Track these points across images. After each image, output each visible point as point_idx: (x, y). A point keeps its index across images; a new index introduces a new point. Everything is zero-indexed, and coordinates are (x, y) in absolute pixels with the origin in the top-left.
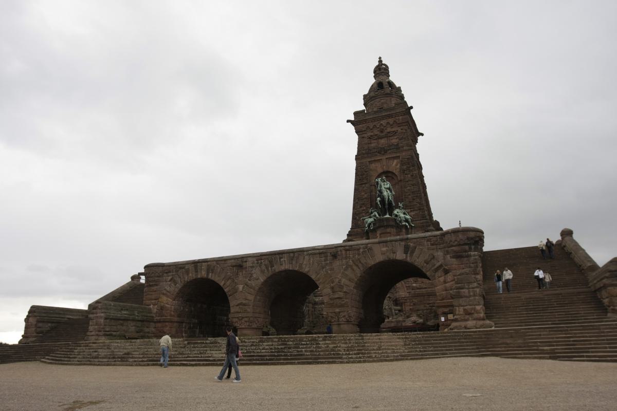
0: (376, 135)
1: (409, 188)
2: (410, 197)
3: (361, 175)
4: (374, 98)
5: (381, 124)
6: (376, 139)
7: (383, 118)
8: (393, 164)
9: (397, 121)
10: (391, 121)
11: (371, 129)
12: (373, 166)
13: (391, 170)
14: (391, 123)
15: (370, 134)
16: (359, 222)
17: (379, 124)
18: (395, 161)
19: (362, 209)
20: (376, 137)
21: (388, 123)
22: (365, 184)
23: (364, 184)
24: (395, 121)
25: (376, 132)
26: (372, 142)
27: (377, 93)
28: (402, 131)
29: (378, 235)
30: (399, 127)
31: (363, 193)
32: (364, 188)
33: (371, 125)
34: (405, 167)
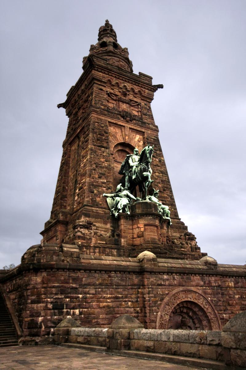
0: (116, 95)
1: (157, 174)
2: (160, 185)
3: (99, 134)
4: (111, 54)
5: (125, 86)
6: (115, 100)
8: (135, 138)
11: (113, 86)
13: (132, 145)
14: (136, 91)
15: (109, 90)
16: (98, 199)
17: (123, 85)
18: (138, 137)
20: (115, 98)
21: (132, 89)
22: (107, 148)
23: (104, 147)
25: (116, 91)
26: (110, 101)
28: (145, 106)
30: (142, 99)
31: (102, 160)
32: (104, 153)
33: (114, 81)
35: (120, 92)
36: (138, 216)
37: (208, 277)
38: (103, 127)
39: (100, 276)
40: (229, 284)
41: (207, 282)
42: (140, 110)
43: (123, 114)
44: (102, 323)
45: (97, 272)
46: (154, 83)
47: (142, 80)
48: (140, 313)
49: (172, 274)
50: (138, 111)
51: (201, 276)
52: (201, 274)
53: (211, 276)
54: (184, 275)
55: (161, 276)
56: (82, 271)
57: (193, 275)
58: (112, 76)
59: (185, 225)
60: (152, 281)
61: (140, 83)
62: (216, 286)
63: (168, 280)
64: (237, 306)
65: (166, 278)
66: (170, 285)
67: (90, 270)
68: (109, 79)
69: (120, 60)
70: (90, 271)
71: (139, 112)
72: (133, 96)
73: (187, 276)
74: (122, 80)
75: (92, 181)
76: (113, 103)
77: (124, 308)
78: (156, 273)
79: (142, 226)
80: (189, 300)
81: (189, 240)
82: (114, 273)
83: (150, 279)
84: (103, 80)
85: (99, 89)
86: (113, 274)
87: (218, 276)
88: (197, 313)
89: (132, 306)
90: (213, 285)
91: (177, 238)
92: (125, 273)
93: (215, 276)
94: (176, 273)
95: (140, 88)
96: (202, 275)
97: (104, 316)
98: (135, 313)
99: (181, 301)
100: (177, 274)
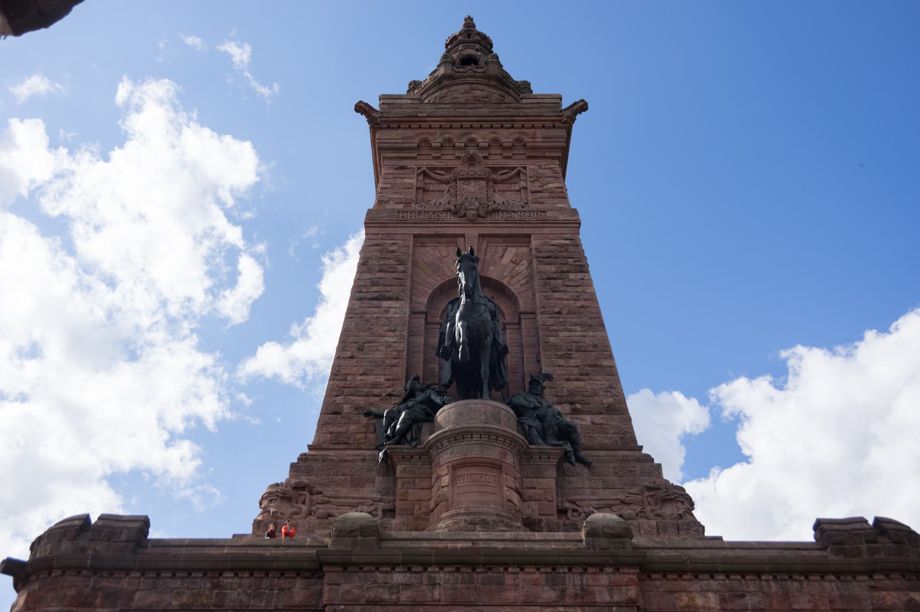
0: (448, 170)
5: (472, 140)
7: (481, 123)
8: (502, 257)
9: (527, 139)
10: (506, 136)
11: (436, 149)
12: (429, 253)
13: (493, 277)
15: (425, 163)
17: (464, 139)
18: (511, 252)
19: (370, 379)
20: (447, 177)
21: (496, 140)
23: (390, 299)
24: (519, 140)
25: (449, 160)
26: (431, 188)
27: (461, 70)
29: (443, 470)
32: (387, 311)
34: (552, 268)
35: (458, 158)
36: (437, 447)
37: (581, 573)
38: (392, 252)
39: (186, 585)
40: (693, 599)
41: (570, 591)
42: (523, 184)
43: (455, 206)
45: (178, 575)
46: (565, 104)
47: (529, 111)
49: (425, 570)
50: (519, 191)
51: (545, 573)
52: (546, 565)
53: (590, 570)
54: (474, 570)
55: (384, 575)
56: (133, 574)
57: (510, 570)
58: (430, 127)
59: (656, 462)
60: (348, 592)
61: (517, 118)
62: (619, 605)
63: (407, 586)
65: (400, 581)
67: (158, 572)
68: (425, 136)
69: (475, 86)
70: (158, 575)
71: (522, 190)
72: (500, 157)
73: (490, 574)
74: (461, 127)
75: (340, 386)
76: (440, 191)
78: (365, 569)
79: (446, 472)
81: (656, 504)
82: (232, 575)
83: (339, 585)
84: (406, 145)
85: (396, 169)
86: (228, 579)
87: (626, 570)
90: (598, 599)
91: (614, 502)
92: (267, 574)
93: (610, 570)
94: (441, 565)
95: (518, 131)
96: (554, 569)
100: (446, 569)
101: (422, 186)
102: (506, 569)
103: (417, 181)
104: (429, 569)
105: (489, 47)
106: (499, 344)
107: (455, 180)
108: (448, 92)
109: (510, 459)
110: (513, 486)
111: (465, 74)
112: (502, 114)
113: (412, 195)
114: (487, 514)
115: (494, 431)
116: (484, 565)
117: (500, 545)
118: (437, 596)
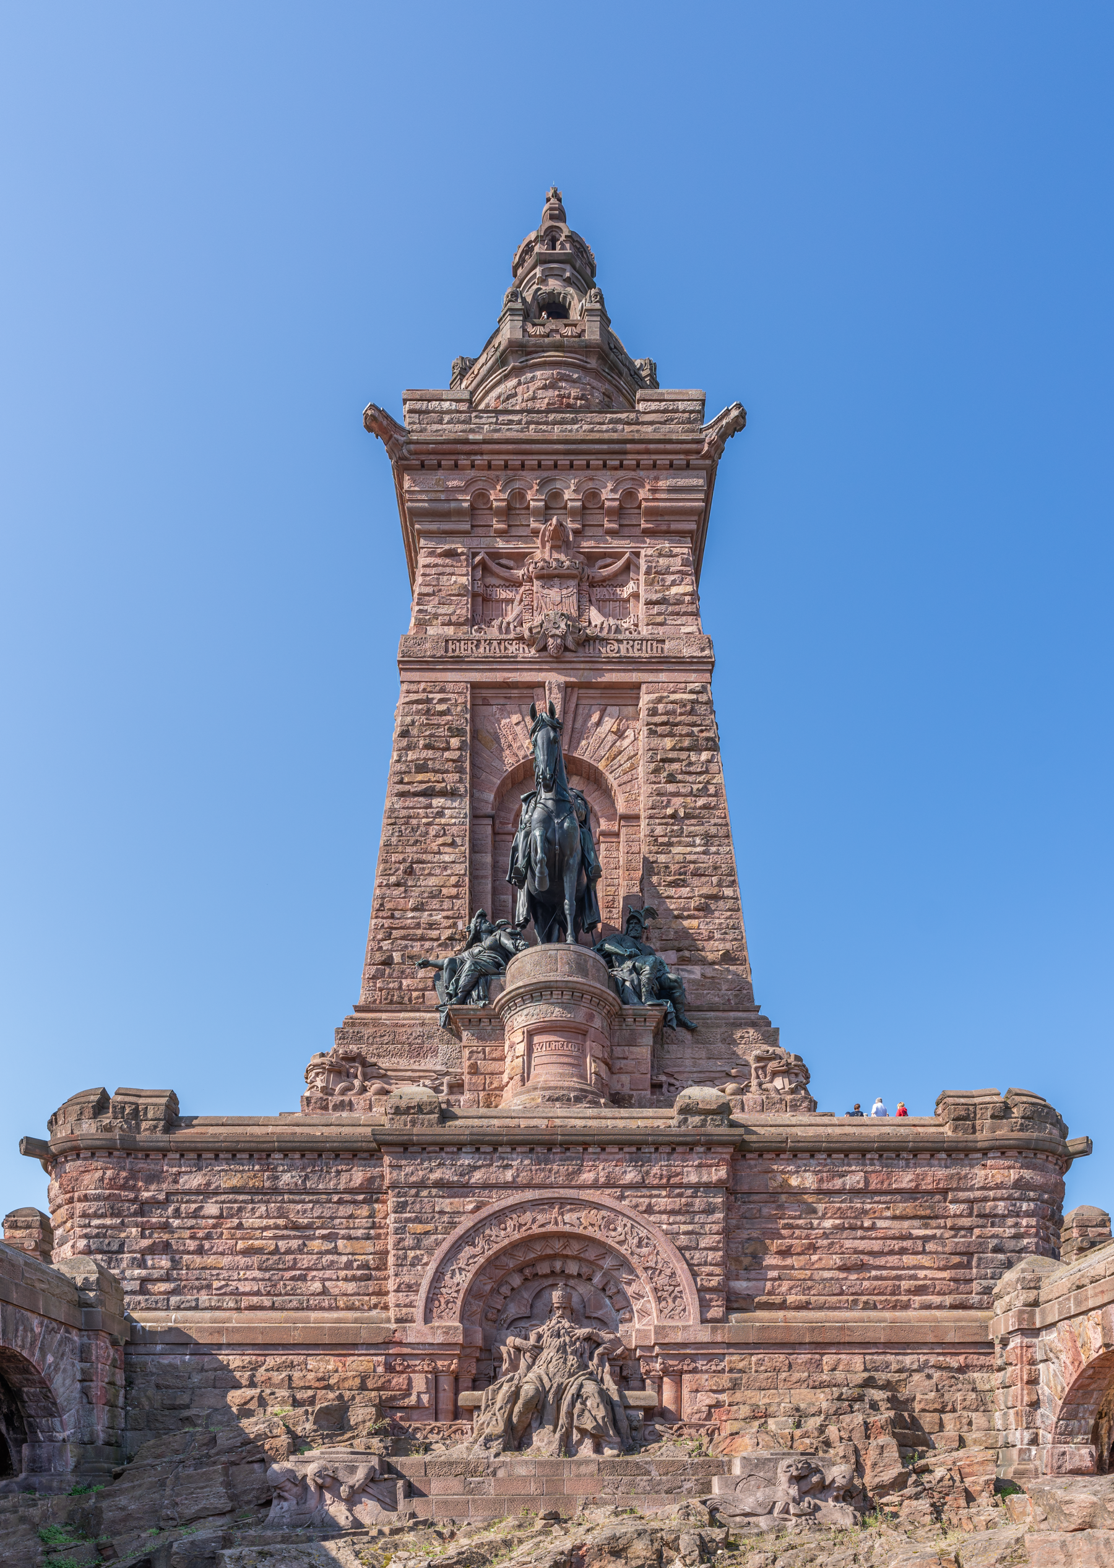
44: (241, 1289)
48: (374, 1269)
54: (550, 1150)
57: (590, 1150)
64: (814, 1258)
66: (486, 1186)
73: (568, 1154)
77: (317, 1253)
79: (521, 1039)
80: (567, 1228)
88: (615, 1273)
89: (348, 1251)
97: (257, 1274)
98: (358, 1268)
99: (530, 1232)
100: (519, 1149)
101: (480, 590)
102: (585, 1149)
103: (473, 580)
104: (500, 1149)
105: (589, 271)
106: (589, 865)
107: (530, 580)
108: (519, 384)
109: (597, 1023)
110: (600, 1056)
111: (546, 340)
112: (606, 436)
113: (462, 609)
114: (569, 1089)
115: (579, 986)
116: (561, 1145)
117: (579, 1123)
118: (509, 1178)
